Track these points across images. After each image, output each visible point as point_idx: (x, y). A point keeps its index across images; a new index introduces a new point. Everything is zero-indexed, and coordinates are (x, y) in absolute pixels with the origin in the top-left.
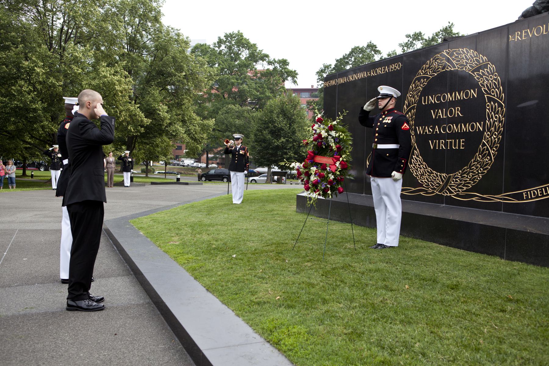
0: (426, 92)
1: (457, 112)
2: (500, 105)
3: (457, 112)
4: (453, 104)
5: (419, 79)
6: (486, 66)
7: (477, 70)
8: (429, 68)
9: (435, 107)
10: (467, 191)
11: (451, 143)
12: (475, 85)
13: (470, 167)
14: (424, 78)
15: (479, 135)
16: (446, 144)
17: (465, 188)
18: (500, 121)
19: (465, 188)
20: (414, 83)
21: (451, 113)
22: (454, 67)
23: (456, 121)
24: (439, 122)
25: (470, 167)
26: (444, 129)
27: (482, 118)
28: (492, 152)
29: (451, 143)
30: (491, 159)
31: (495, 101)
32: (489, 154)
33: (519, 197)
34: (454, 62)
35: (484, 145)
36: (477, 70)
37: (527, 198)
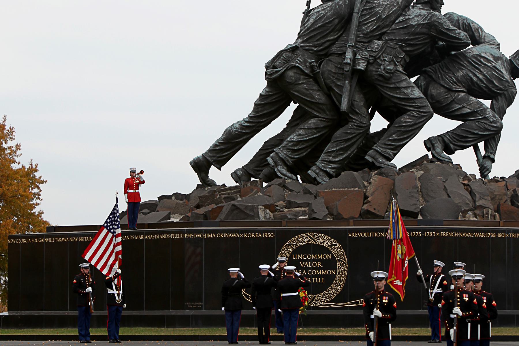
0: (294, 252)
1: (319, 264)
2: (344, 263)
3: (319, 264)
4: (317, 260)
5: (290, 245)
6: (336, 245)
7: (331, 246)
8: (297, 240)
9: (302, 261)
10: (327, 302)
11: (315, 280)
12: (330, 252)
13: (328, 291)
14: (293, 245)
15: (334, 276)
16: (312, 280)
17: (326, 301)
18: (345, 270)
19: (326, 301)
20: (286, 246)
21: (315, 264)
22: (316, 242)
23: (319, 269)
24: (306, 269)
25: (328, 291)
26: (310, 272)
27: (335, 268)
28: (341, 284)
29: (315, 280)
30: (341, 287)
31: (342, 261)
32: (340, 285)
33: (357, 303)
34: (316, 240)
35: (336, 281)
36: (331, 246)
37: (361, 303)
